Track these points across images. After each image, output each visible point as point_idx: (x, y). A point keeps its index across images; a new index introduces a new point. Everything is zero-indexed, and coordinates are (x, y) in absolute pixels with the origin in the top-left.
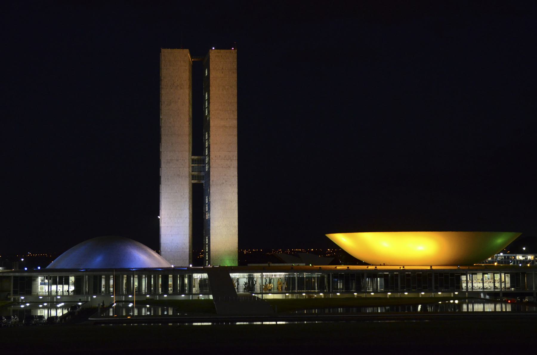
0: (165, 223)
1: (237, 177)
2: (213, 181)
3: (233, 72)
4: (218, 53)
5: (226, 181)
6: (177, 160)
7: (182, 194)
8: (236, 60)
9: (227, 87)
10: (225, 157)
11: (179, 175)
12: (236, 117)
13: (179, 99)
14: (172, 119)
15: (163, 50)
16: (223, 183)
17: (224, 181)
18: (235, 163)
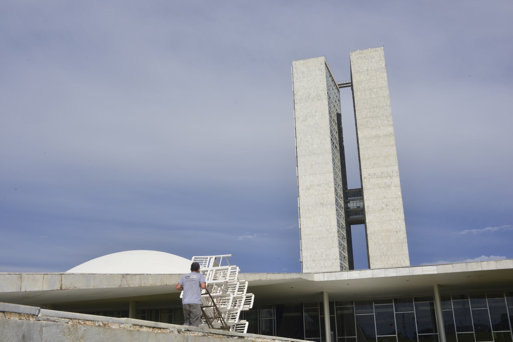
0: (308, 268)
1: (401, 199)
2: (368, 207)
3: (382, 72)
4: (360, 54)
5: (387, 205)
6: (319, 185)
7: (328, 227)
8: (383, 58)
9: (375, 90)
10: (382, 174)
11: (322, 204)
12: (391, 123)
13: (316, 112)
14: (309, 137)
15: (294, 63)
16: (383, 209)
17: (384, 206)
18: (397, 180)
